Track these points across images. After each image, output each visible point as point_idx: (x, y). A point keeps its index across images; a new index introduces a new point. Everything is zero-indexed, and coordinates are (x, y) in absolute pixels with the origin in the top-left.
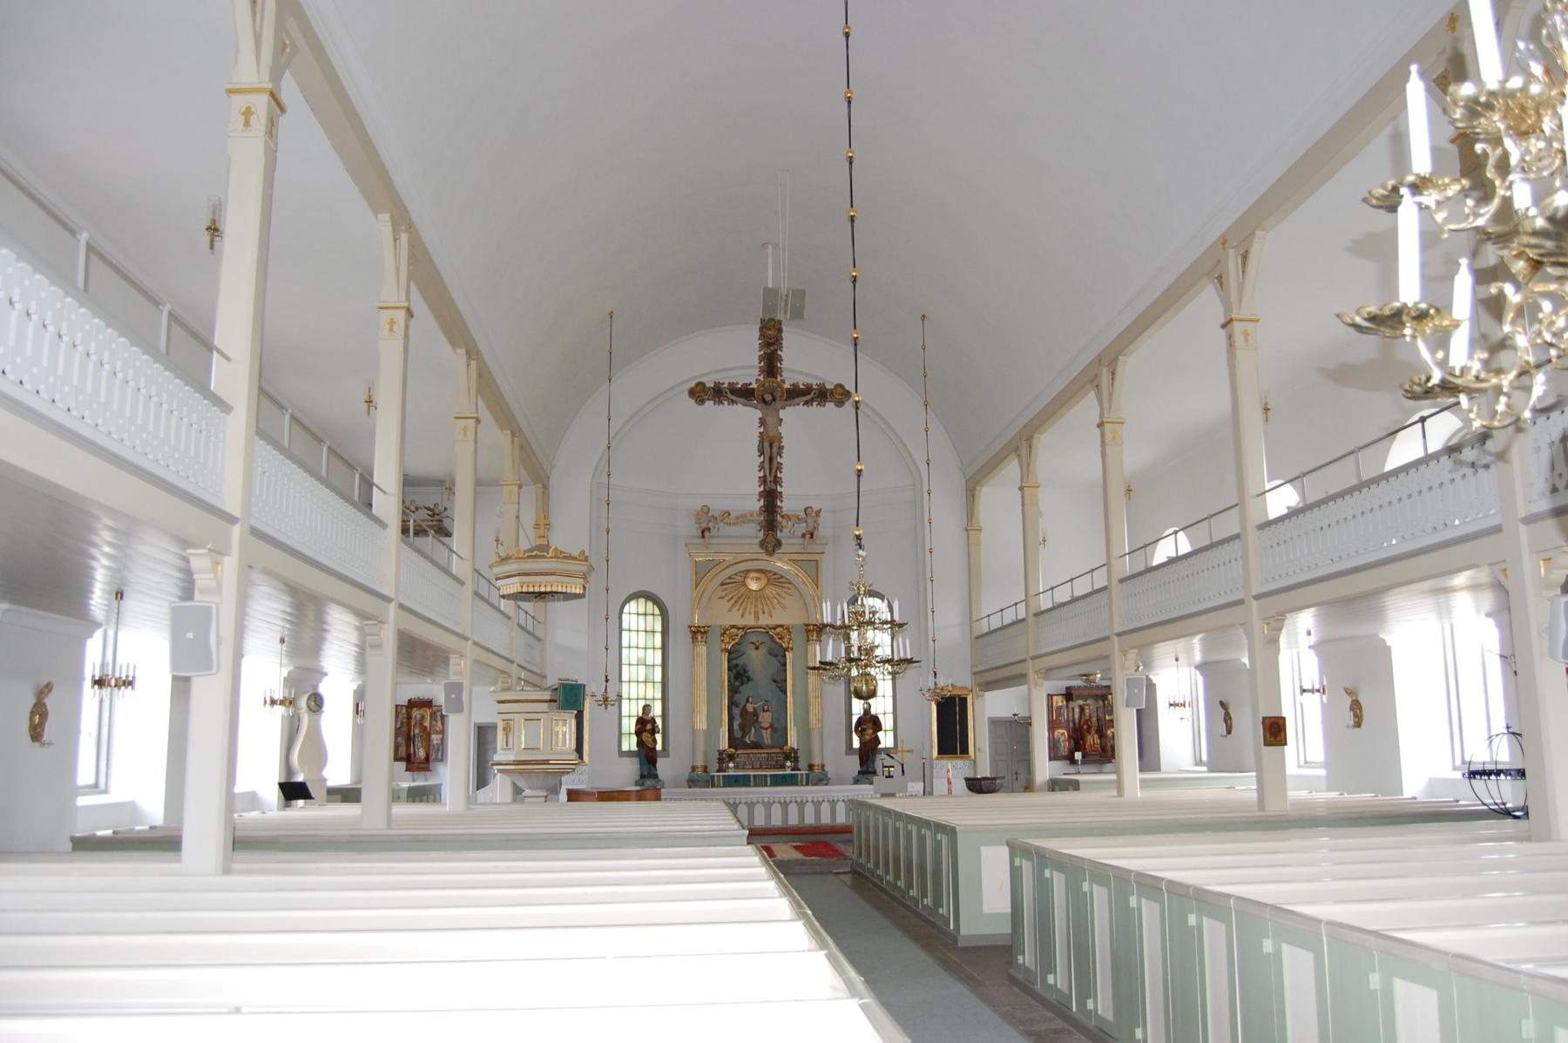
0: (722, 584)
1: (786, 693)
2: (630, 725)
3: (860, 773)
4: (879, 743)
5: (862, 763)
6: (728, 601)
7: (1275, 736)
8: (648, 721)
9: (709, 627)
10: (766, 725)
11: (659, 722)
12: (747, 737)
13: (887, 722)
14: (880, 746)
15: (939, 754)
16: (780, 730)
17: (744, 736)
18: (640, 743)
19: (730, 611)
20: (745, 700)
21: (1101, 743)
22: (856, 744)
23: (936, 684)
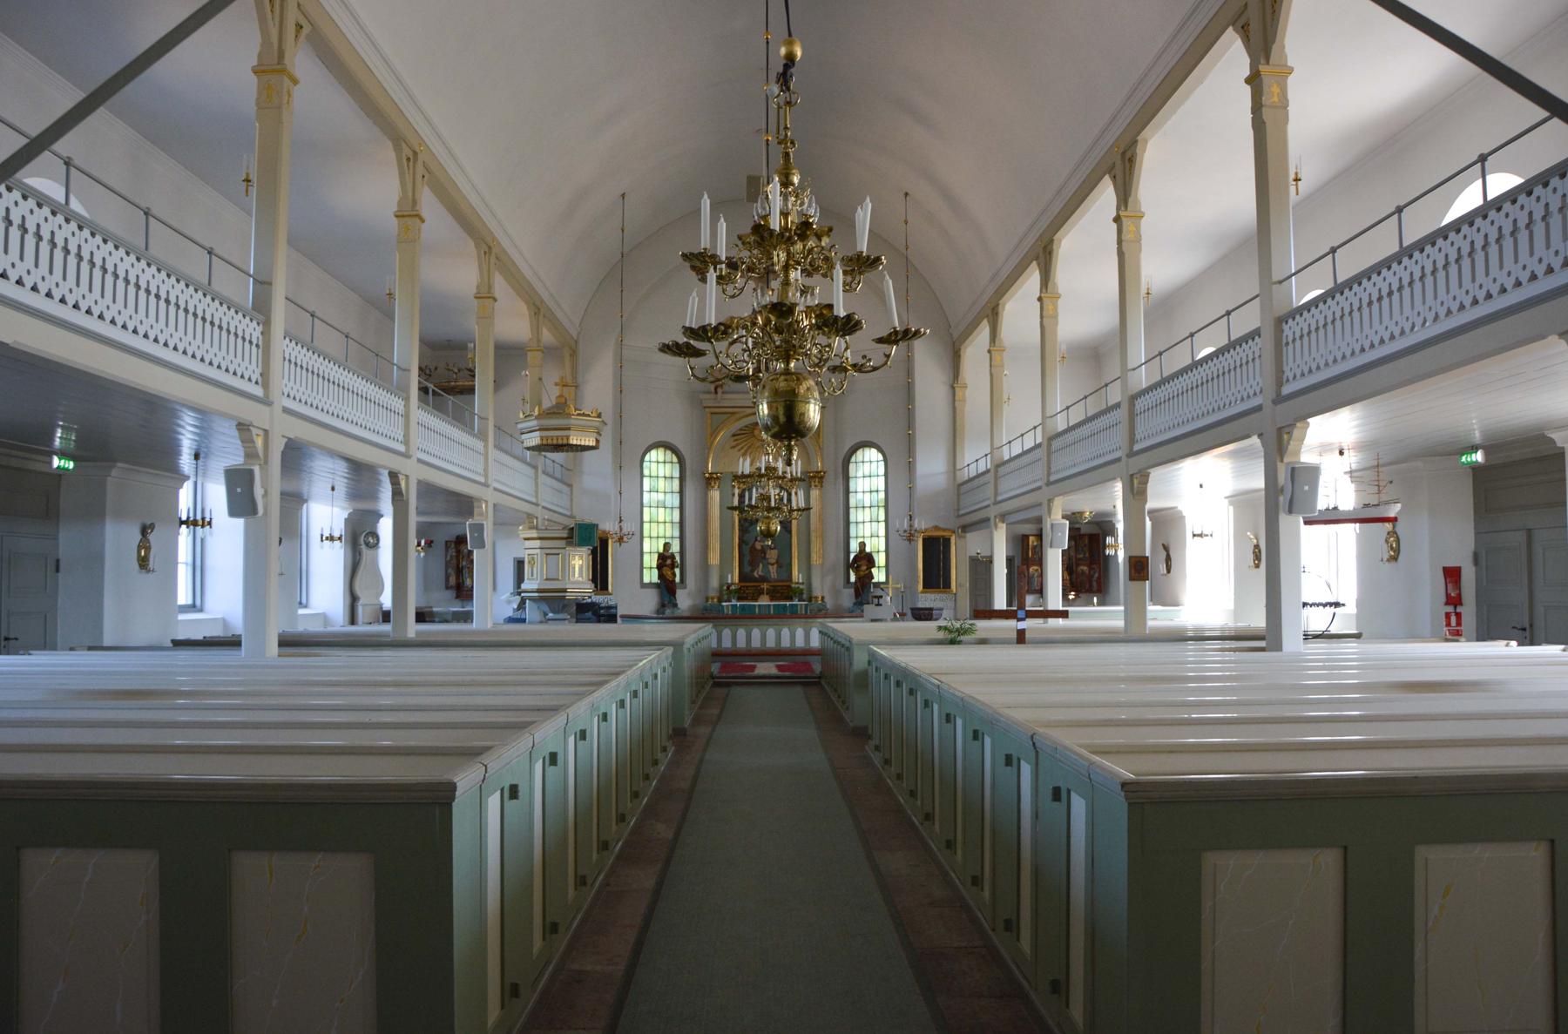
0: (734, 435)
1: (790, 532)
2: (650, 561)
3: (855, 604)
4: (873, 578)
5: (858, 594)
6: (739, 450)
7: (1139, 573)
8: (669, 557)
9: (721, 474)
10: (773, 561)
11: (678, 558)
13: (880, 559)
14: (873, 581)
15: (924, 588)
16: (785, 564)
17: (752, 571)
18: (661, 576)
21: (1071, 579)
22: (853, 578)
23: (911, 526)
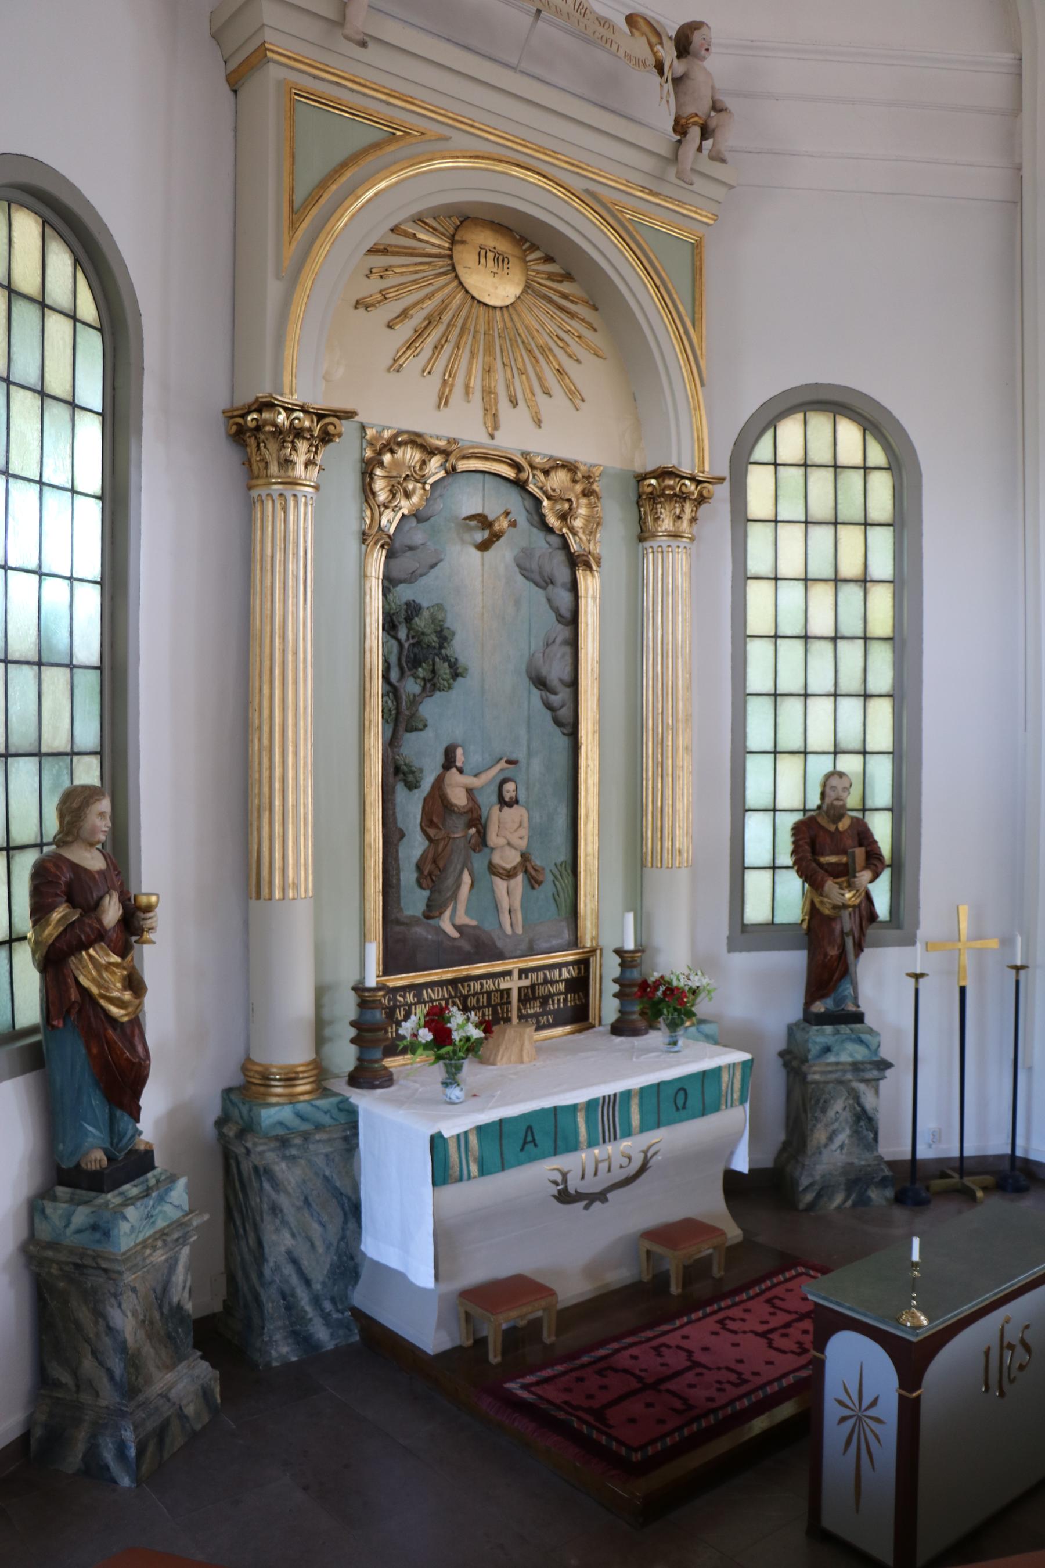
1: (572, 731)
12: (447, 914)
17: (433, 910)
19: (396, 366)
20: (440, 759)
